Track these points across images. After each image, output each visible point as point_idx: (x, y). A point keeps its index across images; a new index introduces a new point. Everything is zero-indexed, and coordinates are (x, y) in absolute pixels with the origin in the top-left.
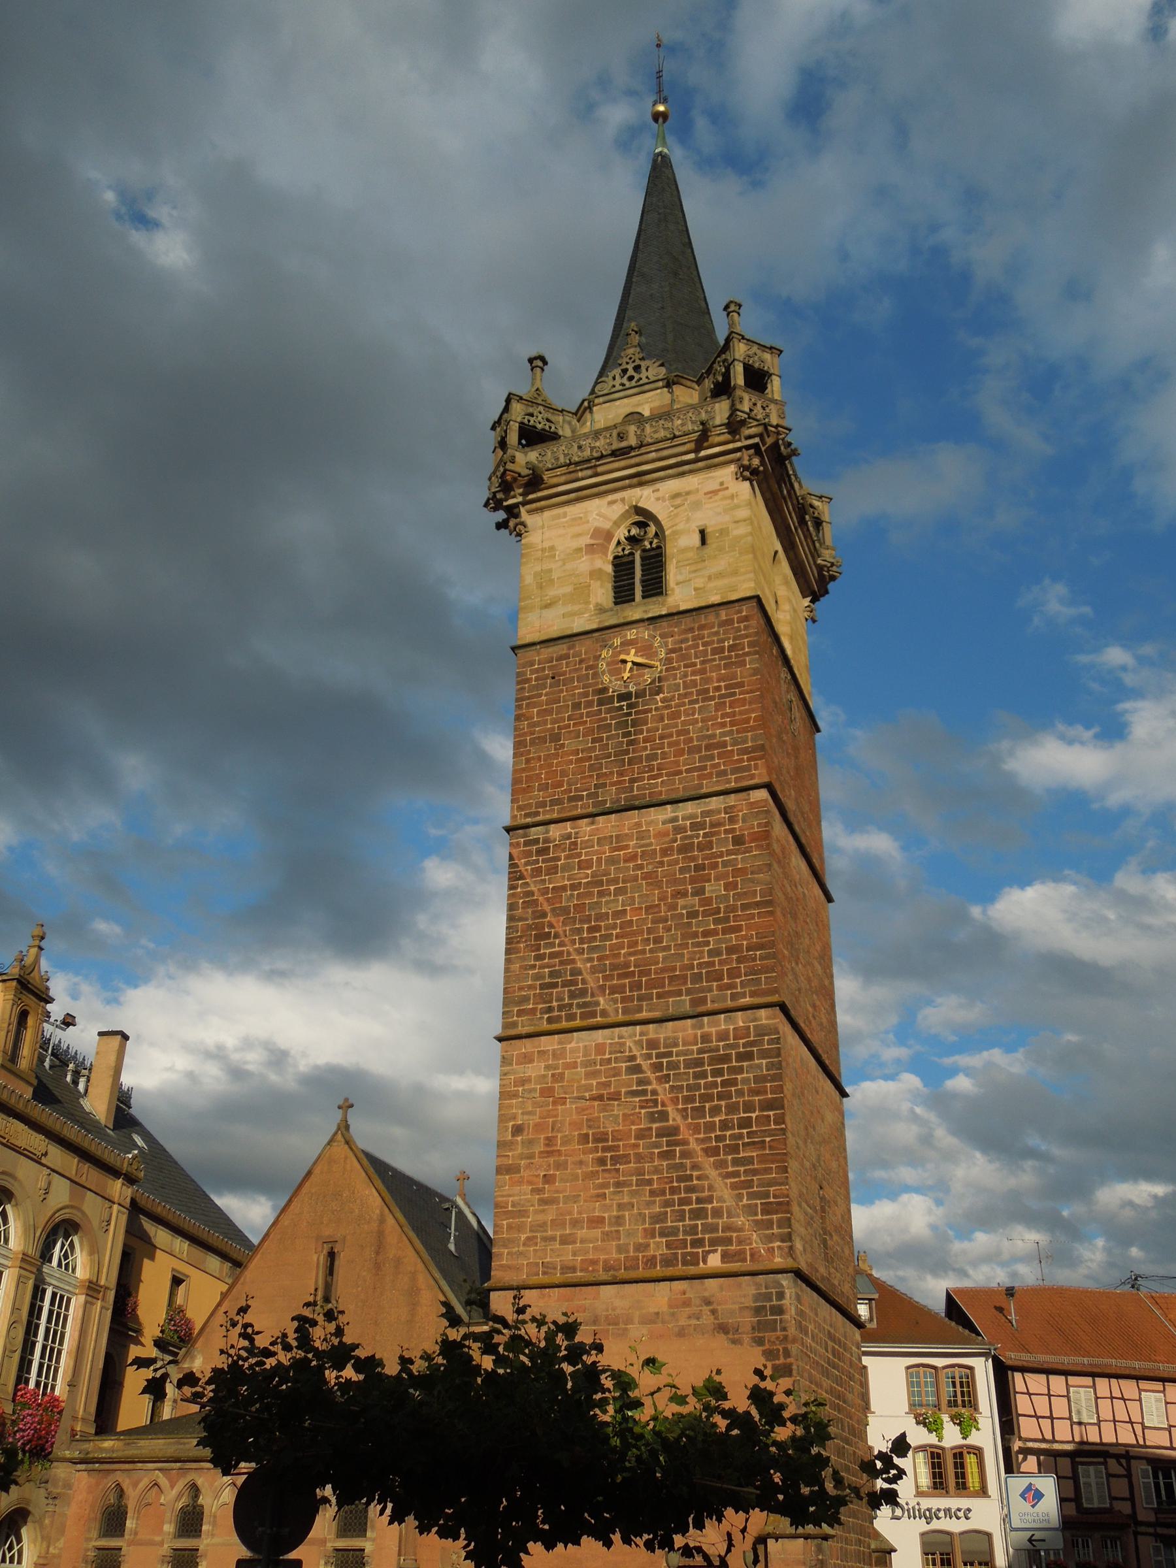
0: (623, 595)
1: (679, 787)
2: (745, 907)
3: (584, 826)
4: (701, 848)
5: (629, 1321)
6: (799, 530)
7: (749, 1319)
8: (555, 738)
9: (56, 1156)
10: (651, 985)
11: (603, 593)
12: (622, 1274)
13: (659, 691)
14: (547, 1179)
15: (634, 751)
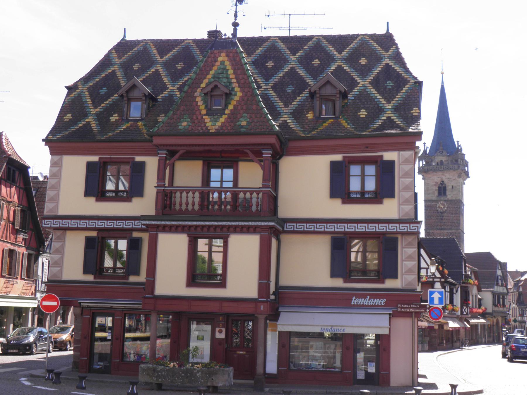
0: (440, 194)
8: (431, 217)
11: (437, 193)
13: (446, 212)
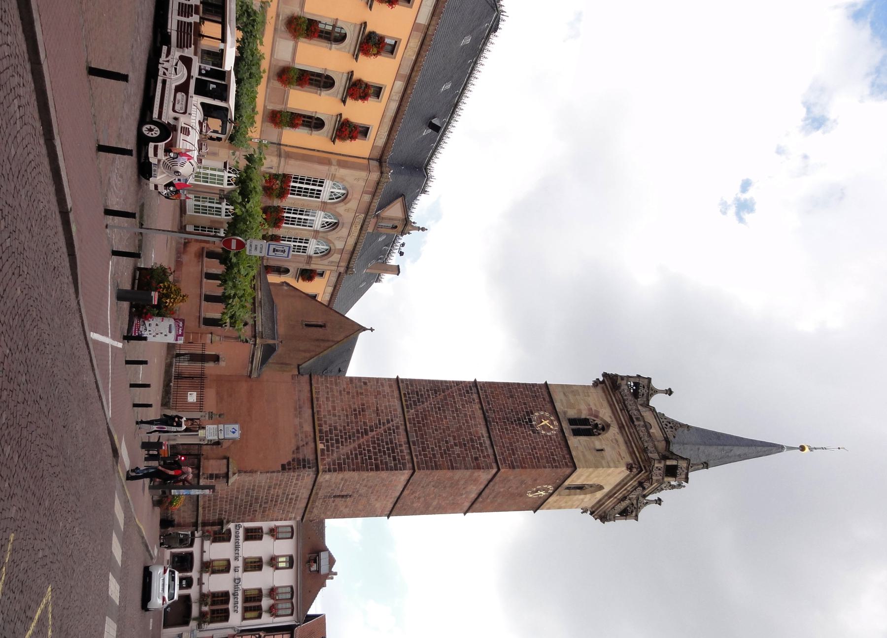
0: (572, 421)
1: (496, 439)
2: (451, 460)
3: (478, 406)
4: (473, 446)
5: (300, 418)
6: (615, 500)
7: (301, 457)
8: (512, 397)
9: (351, 241)
10: (419, 427)
11: (572, 413)
12: (316, 417)
13: (534, 432)
14: (348, 393)
15: (509, 423)
